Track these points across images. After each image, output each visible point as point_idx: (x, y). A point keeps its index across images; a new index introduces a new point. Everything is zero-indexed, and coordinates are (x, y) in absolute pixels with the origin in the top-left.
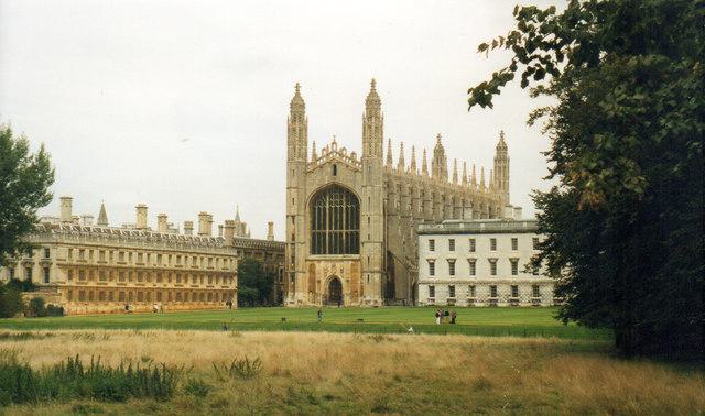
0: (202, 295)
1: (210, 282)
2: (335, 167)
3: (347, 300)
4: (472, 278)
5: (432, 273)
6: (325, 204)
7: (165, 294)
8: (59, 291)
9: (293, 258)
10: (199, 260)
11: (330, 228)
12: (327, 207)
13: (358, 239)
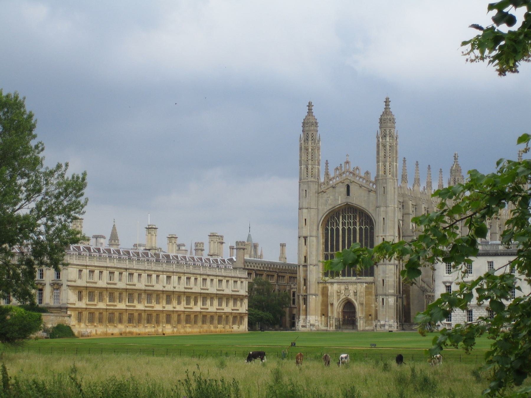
0: (212, 317)
1: (220, 304)
2: (348, 187)
3: (361, 324)
6: (338, 225)
7: (175, 317)
8: (69, 313)
9: (305, 280)
10: (208, 282)
12: (341, 228)
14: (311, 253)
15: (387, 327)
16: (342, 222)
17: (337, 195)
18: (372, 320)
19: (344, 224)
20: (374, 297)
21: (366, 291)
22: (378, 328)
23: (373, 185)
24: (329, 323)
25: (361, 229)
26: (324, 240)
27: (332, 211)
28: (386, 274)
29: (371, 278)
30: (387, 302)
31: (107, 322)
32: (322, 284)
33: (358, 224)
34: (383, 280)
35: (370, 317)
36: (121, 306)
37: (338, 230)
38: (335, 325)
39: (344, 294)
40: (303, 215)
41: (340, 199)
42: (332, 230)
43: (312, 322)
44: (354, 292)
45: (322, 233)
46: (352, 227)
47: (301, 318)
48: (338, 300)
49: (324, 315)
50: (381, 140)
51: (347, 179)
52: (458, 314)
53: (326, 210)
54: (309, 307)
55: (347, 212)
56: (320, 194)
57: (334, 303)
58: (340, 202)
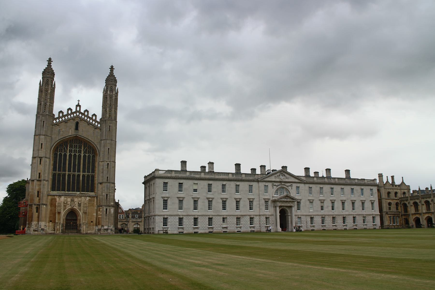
2: (77, 124)
3: (84, 229)
5: (165, 207)
11: (69, 170)
12: (68, 154)
13: (93, 181)
14: (45, 171)
15: (109, 231)
16: (70, 150)
19: (71, 151)
20: (96, 208)
22: (102, 232)
23: (98, 124)
24: (56, 228)
25: (85, 156)
26: (53, 163)
27: (62, 141)
28: (110, 190)
29: (92, 193)
30: (110, 211)
32: (51, 196)
33: (82, 152)
34: (107, 195)
35: (92, 223)
37: (65, 155)
38: (62, 230)
39: (70, 205)
40: (40, 140)
41: (70, 132)
42: (61, 155)
43: (42, 227)
44: (79, 203)
45: (53, 157)
46: (77, 154)
47: (33, 224)
48: (64, 210)
49: (51, 221)
50: (109, 92)
52: (173, 220)
53: (57, 139)
54: (41, 214)
55: (74, 143)
56: (54, 126)
57: (61, 212)
58: (70, 135)
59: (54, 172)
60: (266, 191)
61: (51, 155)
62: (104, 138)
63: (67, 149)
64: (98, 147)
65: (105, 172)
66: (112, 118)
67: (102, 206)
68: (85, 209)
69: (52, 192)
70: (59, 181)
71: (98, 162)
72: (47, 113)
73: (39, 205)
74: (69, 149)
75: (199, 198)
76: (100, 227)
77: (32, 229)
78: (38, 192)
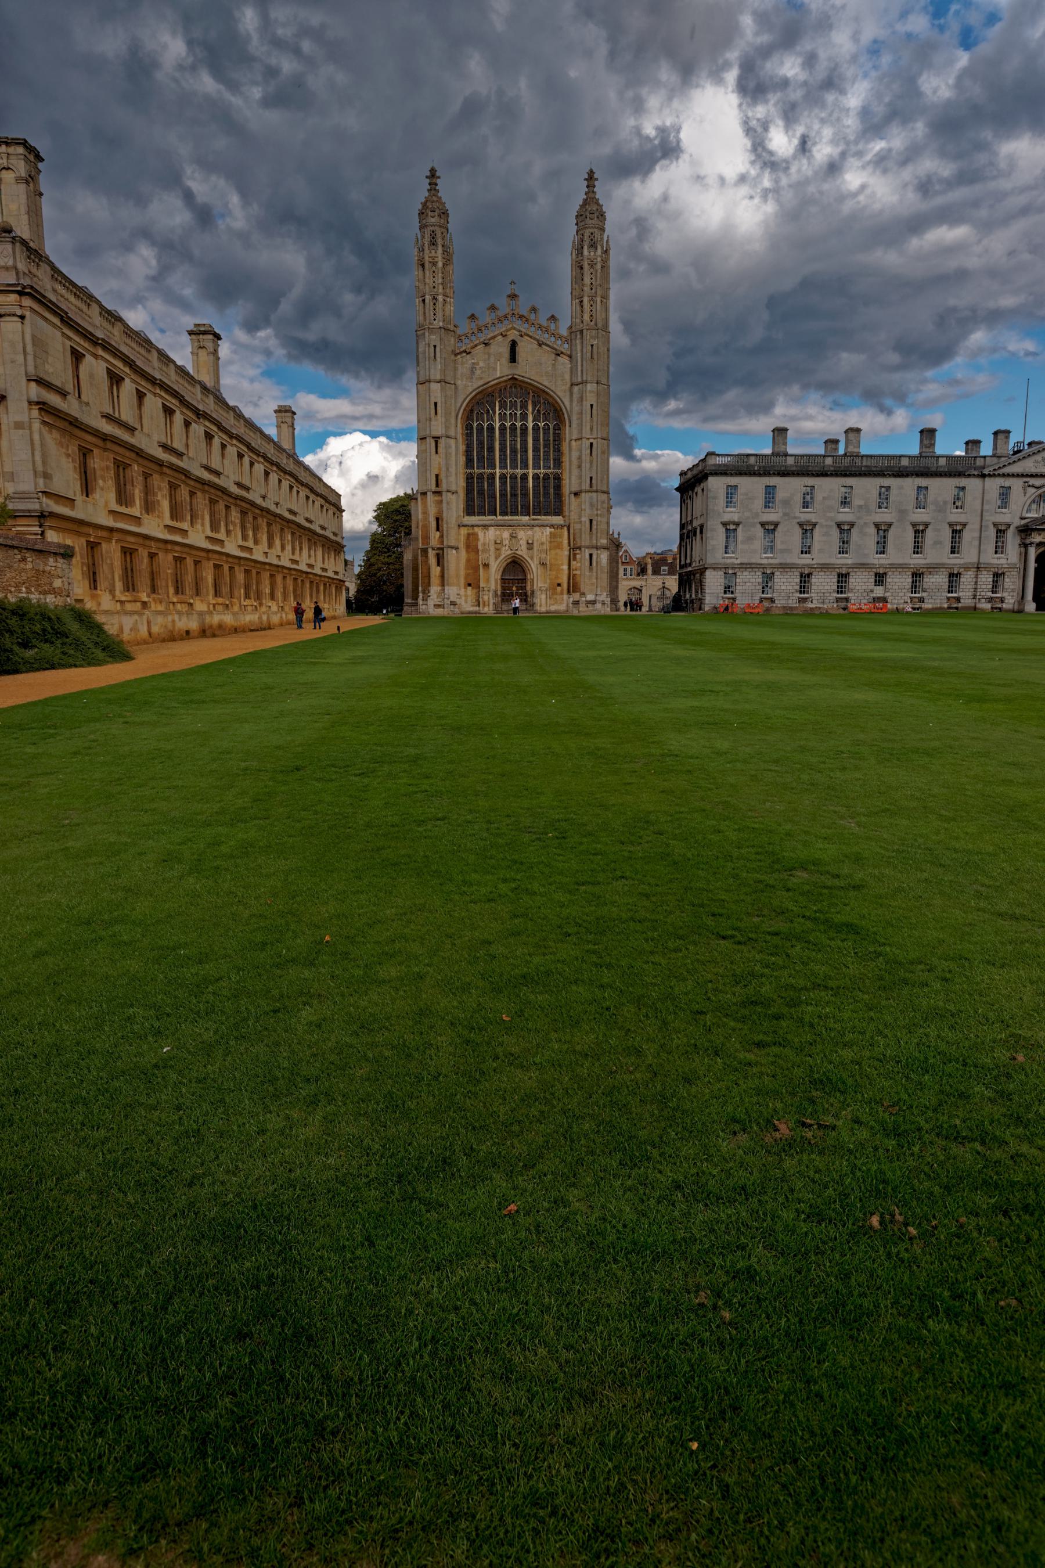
4: (806, 559)
11: (503, 466)
12: (497, 425)
13: (558, 488)
14: (448, 469)
15: (598, 606)
17: (492, 359)
18: (562, 593)
19: (502, 417)
20: (567, 553)
21: (550, 542)
22: (582, 608)
25: (536, 428)
31: (171, 590)
33: (530, 418)
34: (591, 521)
35: (559, 589)
36: (198, 536)
37: (491, 428)
42: (480, 429)
43: (452, 599)
46: (518, 424)
48: (496, 558)
49: (469, 585)
50: (586, 252)
51: (514, 328)
53: (470, 389)
59: (469, 471)
60: (1004, 504)
61: (459, 430)
62: (580, 380)
63: (494, 413)
64: (567, 404)
65: (586, 465)
66: (596, 324)
67: (580, 548)
68: (543, 556)
69: (467, 518)
70: (481, 493)
71: (567, 440)
72: (441, 324)
73: (442, 549)
74: (498, 412)
75: (815, 525)
76: (576, 596)
77: (431, 602)
78: (437, 519)
